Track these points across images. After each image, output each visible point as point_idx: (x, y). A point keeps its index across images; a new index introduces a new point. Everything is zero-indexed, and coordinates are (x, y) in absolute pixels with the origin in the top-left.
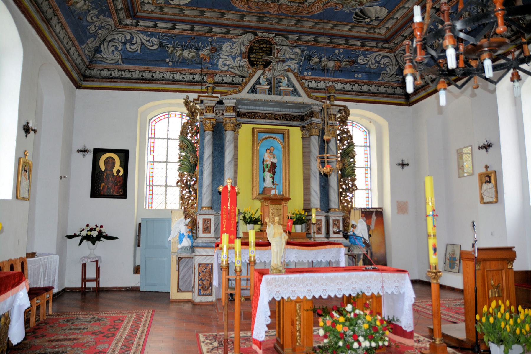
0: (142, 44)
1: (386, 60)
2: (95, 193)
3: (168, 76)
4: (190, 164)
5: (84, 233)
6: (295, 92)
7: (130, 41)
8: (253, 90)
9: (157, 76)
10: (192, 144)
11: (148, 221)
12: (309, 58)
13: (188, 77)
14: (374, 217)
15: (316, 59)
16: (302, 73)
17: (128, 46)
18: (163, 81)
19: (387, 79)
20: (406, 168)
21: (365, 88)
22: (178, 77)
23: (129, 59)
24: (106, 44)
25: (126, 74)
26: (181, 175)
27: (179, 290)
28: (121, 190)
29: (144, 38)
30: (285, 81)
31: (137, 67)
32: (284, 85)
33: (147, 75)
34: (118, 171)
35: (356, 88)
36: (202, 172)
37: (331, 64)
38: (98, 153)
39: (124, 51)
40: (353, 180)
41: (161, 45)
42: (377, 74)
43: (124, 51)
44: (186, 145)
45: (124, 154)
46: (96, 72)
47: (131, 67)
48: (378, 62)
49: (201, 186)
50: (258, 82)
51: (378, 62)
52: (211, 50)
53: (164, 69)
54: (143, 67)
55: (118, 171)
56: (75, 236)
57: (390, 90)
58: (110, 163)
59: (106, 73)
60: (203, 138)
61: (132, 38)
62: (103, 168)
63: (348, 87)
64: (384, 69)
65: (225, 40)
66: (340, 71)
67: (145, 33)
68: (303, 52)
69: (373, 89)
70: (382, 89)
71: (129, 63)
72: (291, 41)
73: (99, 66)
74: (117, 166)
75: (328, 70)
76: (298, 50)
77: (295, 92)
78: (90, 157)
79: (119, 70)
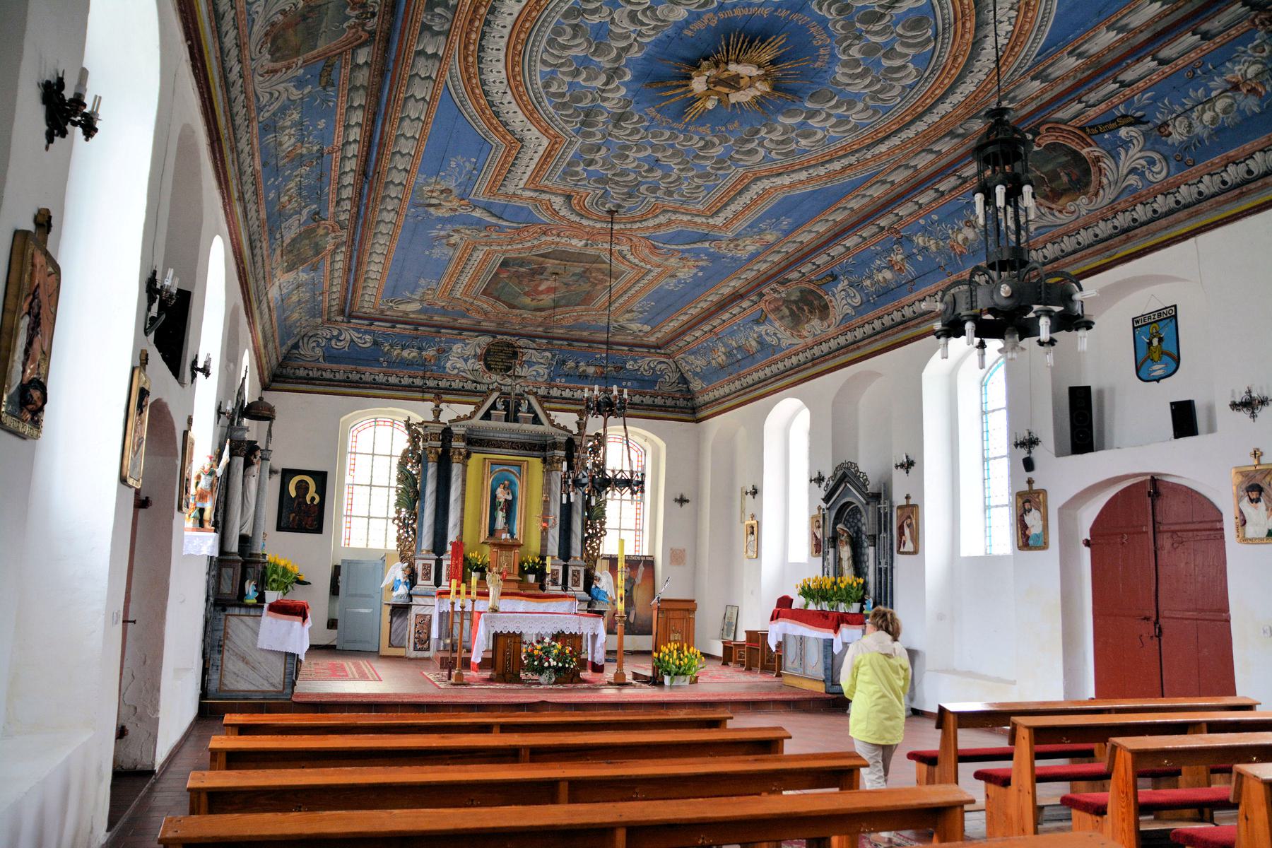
0: (352, 341)
1: (664, 366)
3: (381, 378)
4: (410, 496)
6: (536, 420)
7: (337, 338)
8: (487, 416)
9: (367, 378)
10: (412, 475)
11: (349, 563)
12: (564, 362)
13: (406, 381)
14: (641, 568)
15: (571, 364)
16: (552, 379)
17: (333, 342)
18: (375, 385)
19: (667, 389)
20: (686, 505)
22: (393, 380)
24: (306, 339)
25: (328, 375)
26: (398, 512)
27: (391, 645)
29: (355, 335)
30: (524, 407)
31: (342, 367)
32: (523, 413)
33: (354, 376)
34: (313, 499)
37: (591, 370)
38: (287, 474)
39: (328, 348)
40: (603, 523)
41: (375, 343)
43: (328, 348)
44: (405, 477)
45: (321, 478)
46: (289, 371)
47: (335, 366)
48: (653, 369)
49: (421, 525)
50: (493, 406)
52: (438, 351)
53: (377, 370)
54: (350, 367)
55: (313, 499)
57: (669, 402)
58: (302, 487)
59: (302, 373)
60: (425, 470)
61: (340, 334)
62: (293, 493)
64: (662, 376)
65: (455, 342)
67: (358, 331)
68: (554, 356)
69: (648, 400)
70: (659, 401)
71: (332, 362)
72: (539, 344)
73: (295, 364)
75: (587, 377)
76: (548, 354)
77: (536, 420)
78: (277, 479)
79: (318, 369)
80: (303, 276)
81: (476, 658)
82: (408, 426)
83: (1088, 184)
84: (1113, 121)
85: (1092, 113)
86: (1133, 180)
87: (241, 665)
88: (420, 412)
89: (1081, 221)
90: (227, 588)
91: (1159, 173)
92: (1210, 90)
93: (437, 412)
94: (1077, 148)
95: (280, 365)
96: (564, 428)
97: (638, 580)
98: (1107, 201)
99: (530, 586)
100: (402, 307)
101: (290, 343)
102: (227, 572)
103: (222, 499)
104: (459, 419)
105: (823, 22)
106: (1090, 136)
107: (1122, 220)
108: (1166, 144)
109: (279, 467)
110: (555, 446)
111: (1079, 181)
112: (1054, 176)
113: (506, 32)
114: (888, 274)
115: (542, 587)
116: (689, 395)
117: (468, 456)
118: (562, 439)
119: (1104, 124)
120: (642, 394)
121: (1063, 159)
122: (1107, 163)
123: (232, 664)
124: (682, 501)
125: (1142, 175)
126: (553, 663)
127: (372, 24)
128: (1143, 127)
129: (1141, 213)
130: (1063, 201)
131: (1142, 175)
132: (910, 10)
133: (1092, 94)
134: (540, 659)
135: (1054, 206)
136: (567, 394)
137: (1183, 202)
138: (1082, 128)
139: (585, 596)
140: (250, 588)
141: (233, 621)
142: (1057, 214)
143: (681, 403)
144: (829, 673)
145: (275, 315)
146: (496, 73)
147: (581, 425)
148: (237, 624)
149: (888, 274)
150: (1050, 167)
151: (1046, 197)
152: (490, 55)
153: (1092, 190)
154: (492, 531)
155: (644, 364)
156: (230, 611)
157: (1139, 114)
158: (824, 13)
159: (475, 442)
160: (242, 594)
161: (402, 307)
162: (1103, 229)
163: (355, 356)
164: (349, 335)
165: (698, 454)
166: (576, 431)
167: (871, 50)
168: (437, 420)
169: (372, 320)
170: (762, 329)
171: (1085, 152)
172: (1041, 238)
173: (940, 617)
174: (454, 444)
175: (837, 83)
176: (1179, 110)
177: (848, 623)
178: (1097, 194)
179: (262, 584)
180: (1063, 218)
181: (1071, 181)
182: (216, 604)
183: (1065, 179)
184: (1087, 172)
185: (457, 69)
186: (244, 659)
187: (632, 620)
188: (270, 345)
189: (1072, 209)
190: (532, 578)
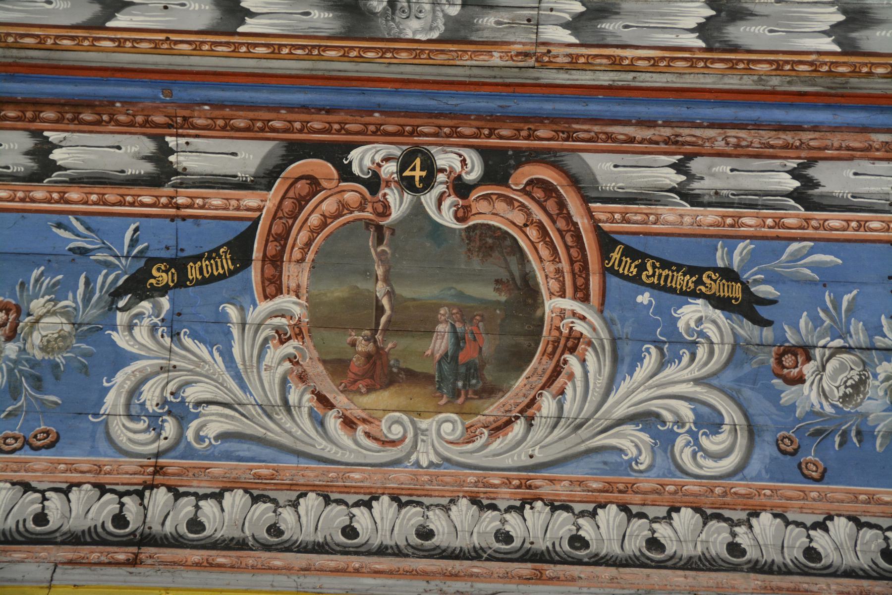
84: (692, 271)
85: (675, 215)
86: (632, 441)
89: (399, 477)
98: (519, 458)
106: (607, 271)
107: (536, 527)
108: (774, 396)
111: (473, 370)
112: (416, 322)
119: (666, 264)
122: (588, 368)
128: (747, 330)
129: (607, 530)
133: (723, 166)
135: (340, 400)
137: (752, 554)
138: (606, 242)
142: (333, 423)
150: (427, 292)
151: (337, 366)
153: (493, 409)
157: (764, 290)
172: (219, 468)
176: (858, 335)
178: (499, 428)
180: (344, 445)
181: (451, 358)
184: (518, 359)
189: (396, 432)
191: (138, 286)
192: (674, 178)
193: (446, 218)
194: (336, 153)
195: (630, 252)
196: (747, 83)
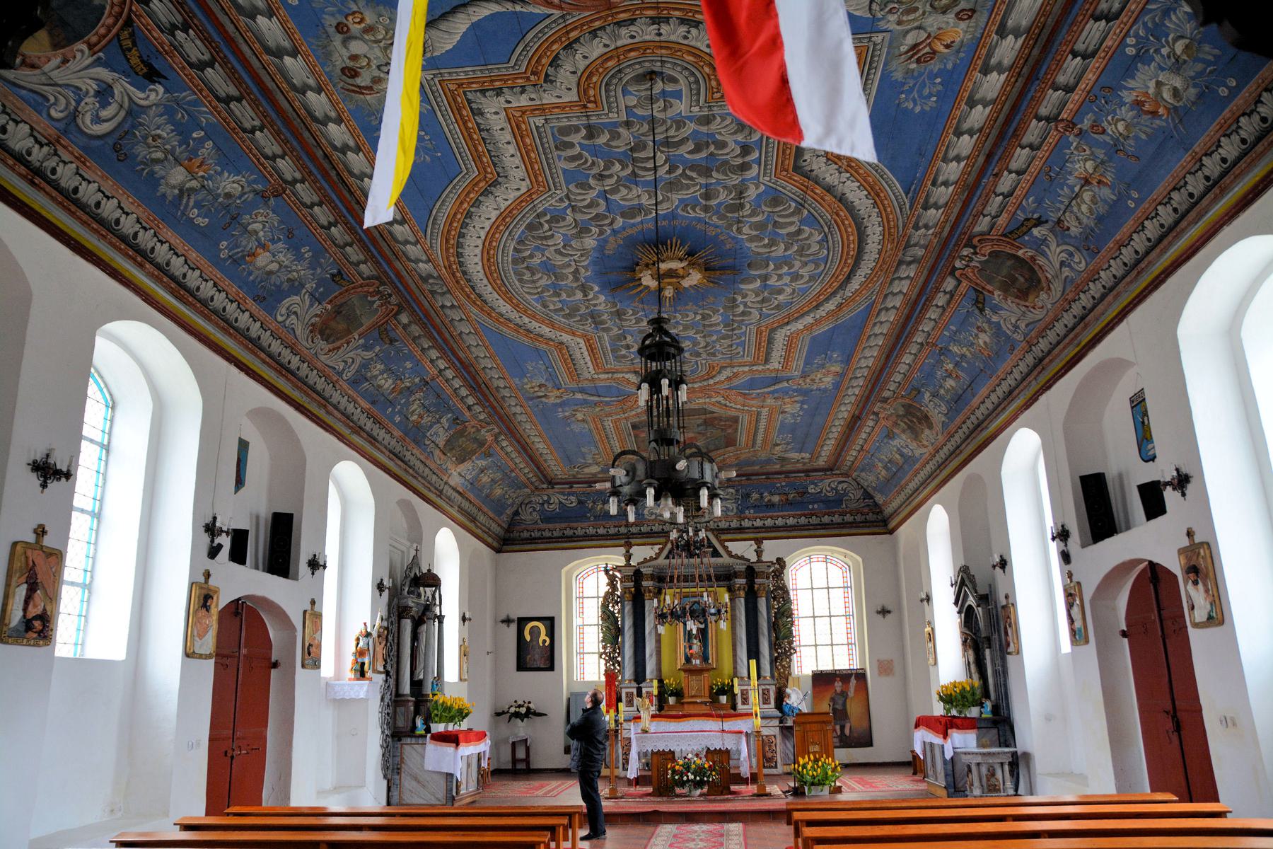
1: (845, 485)
2: (522, 666)
3: (591, 531)
5: (512, 710)
6: (716, 554)
7: (548, 502)
9: (579, 532)
10: (613, 613)
12: (748, 495)
13: (612, 531)
14: (853, 681)
15: (755, 496)
16: (742, 512)
19: (853, 506)
20: (889, 616)
21: (826, 519)
22: (601, 531)
23: (548, 518)
25: (547, 534)
26: (604, 647)
28: (549, 662)
29: (562, 498)
31: (557, 525)
33: (569, 532)
34: (544, 641)
35: (814, 520)
36: (623, 641)
37: (776, 499)
38: (522, 622)
39: (542, 512)
41: (580, 502)
42: (839, 501)
43: (542, 512)
45: (550, 622)
46: (515, 534)
47: (550, 526)
48: (836, 489)
49: (623, 658)
51: (836, 489)
54: (563, 525)
55: (544, 641)
56: (503, 713)
57: (859, 518)
59: (526, 535)
60: (623, 606)
62: (528, 638)
63: (803, 520)
64: (846, 494)
66: (789, 504)
67: (563, 494)
68: (737, 491)
69: (837, 519)
70: (848, 518)
74: (543, 636)
75: (773, 505)
76: (731, 490)
77: (716, 554)
78: (514, 627)
80: (481, 463)
81: (632, 773)
82: (607, 571)
83: (1039, 281)
84: (1022, 225)
85: (1002, 220)
86: (1066, 272)
87: (414, 783)
88: (616, 558)
90: (401, 723)
91: (1080, 263)
92: (1071, 188)
93: (628, 557)
94: (1013, 252)
95: (508, 531)
96: (742, 558)
97: (851, 693)
98: (1059, 294)
99: (722, 707)
100: (586, 470)
101: (509, 511)
102: (401, 710)
103: (394, 652)
104: (646, 561)
105: (699, 220)
107: (1076, 309)
108: (1070, 237)
109: (514, 616)
110: (736, 575)
112: (1014, 280)
113: (485, 281)
114: (950, 383)
115: (734, 707)
116: (877, 509)
117: (659, 592)
118: (741, 567)
120: (832, 514)
121: (1009, 263)
122: (1041, 261)
123: (408, 783)
124: (884, 612)
125: (1069, 266)
126: (691, 777)
127: (394, 300)
129: (1085, 300)
130: (1031, 298)
131: (1069, 266)
132: (759, 196)
134: (681, 774)
136: (758, 523)
139: (778, 713)
140: (419, 722)
141: (407, 749)
143: (871, 517)
144: (950, 779)
145: (472, 497)
146: (504, 307)
147: (759, 553)
148: (409, 750)
149: (950, 383)
150: (1004, 272)
151: (1018, 297)
152: (489, 298)
154: (688, 660)
155: (826, 485)
156: (405, 740)
157: (1036, 216)
158: (693, 215)
159: (661, 579)
160: (414, 727)
161: (586, 470)
162: (1068, 319)
163: (565, 515)
164: (556, 499)
165: (896, 564)
166: (754, 558)
167: (760, 226)
168: (628, 565)
169: (571, 484)
170: (895, 442)
171: (1020, 253)
173: (1048, 718)
174: (645, 583)
175: (759, 254)
176: (1063, 207)
177: (958, 728)
178: (1049, 289)
179: (428, 721)
180: (1039, 314)
182: (393, 736)
183: (1022, 279)
184: (1032, 270)
185: (475, 311)
186: (416, 779)
187: (847, 732)
188: (481, 518)
189: (1040, 304)
190: (723, 699)
191: (982, 310)
192: (988, 218)
193: (983, 258)
194: (954, 269)
195: (1011, 233)
196: (959, 205)
